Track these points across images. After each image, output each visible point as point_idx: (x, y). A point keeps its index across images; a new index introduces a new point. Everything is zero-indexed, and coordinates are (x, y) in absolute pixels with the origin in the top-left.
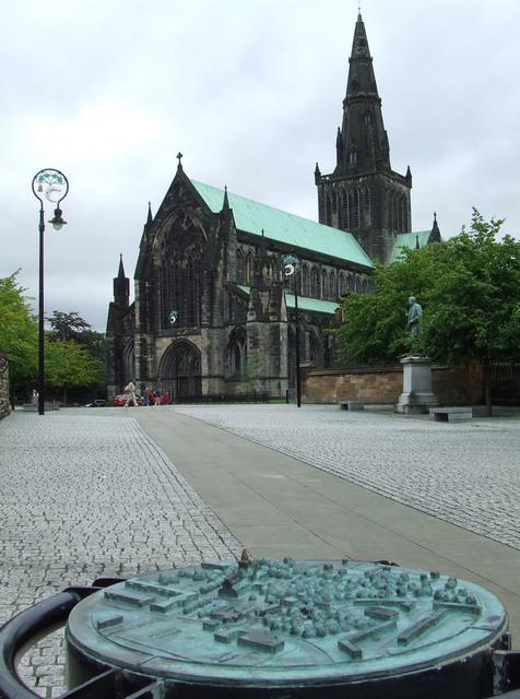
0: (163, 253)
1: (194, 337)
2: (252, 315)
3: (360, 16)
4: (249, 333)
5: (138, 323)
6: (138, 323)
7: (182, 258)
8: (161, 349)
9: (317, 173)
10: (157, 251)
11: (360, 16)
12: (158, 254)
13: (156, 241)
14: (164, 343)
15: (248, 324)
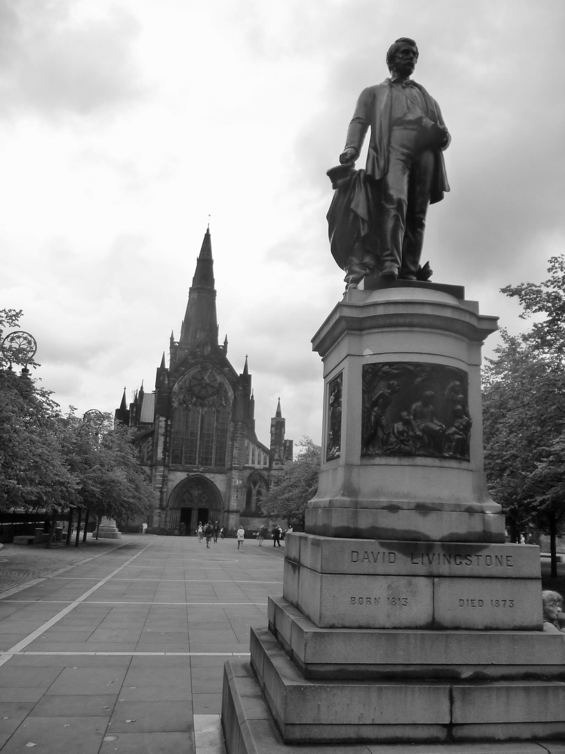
0: (181, 397)
1: (212, 475)
2: (276, 464)
3: (208, 230)
4: (273, 480)
5: (160, 455)
6: (160, 455)
7: (203, 406)
8: (173, 481)
9: (172, 338)
10: (175, 393)
11: (208, 230)
12: (175, 396)
13: (176, 386)
14: (179, 477)
15: (273, 472)
